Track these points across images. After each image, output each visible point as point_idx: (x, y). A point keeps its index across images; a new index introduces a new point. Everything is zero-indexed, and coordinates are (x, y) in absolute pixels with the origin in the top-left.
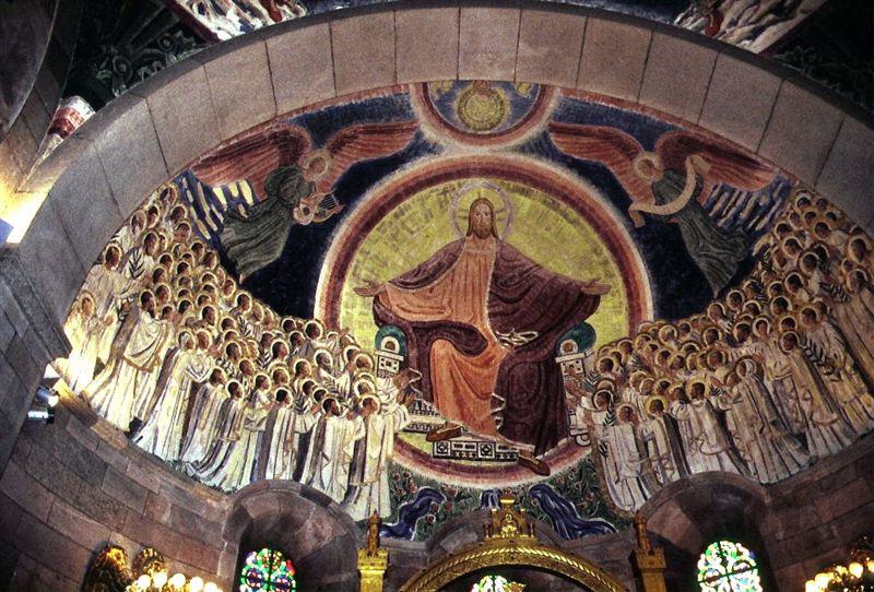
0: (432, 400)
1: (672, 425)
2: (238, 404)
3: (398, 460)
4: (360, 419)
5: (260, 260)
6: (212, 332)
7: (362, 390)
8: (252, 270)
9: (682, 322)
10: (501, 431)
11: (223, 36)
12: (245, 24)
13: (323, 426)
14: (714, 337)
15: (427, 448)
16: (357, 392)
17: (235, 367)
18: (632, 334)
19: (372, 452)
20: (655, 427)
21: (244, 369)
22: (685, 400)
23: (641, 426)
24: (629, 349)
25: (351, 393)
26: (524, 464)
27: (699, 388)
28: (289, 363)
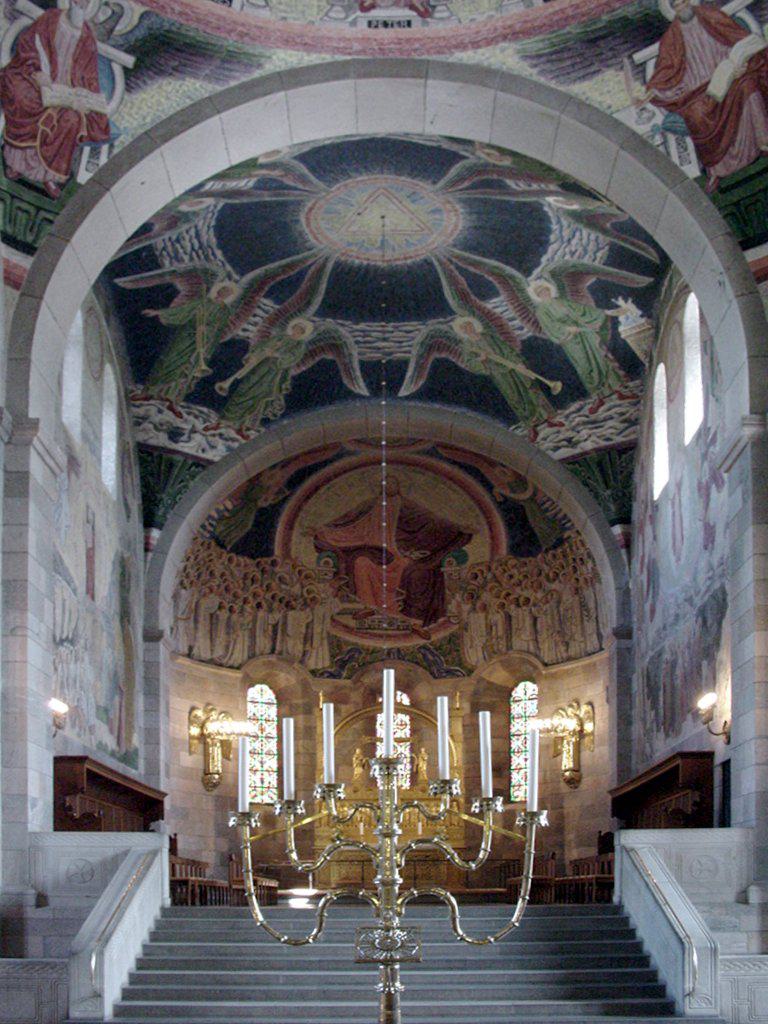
0: (355, 593)
1: (509, 618)
2: (235, 617)
3: (334, 632)
4: (308, 610)
5: (237, 536)
6: (217, 581)
7: (309, 592)
8: (234, 541)
9: (523, 559)
10: (402, 611)
11: (217, 459)
12: (229, 449)
13: (285, 617)
14: (540, 574)
15: (352, 623)
16: (305, 594)
17: (229, 597)
18: (492, 559)
19: (317, 629)
20: (498, 618)
21: (236, 596)
22: (518, 605)
23: (490, 616)
24: (489, 569)
25: (302, 596)
26: (415, 631)
27: (528, 600)
28: (261, 586)
